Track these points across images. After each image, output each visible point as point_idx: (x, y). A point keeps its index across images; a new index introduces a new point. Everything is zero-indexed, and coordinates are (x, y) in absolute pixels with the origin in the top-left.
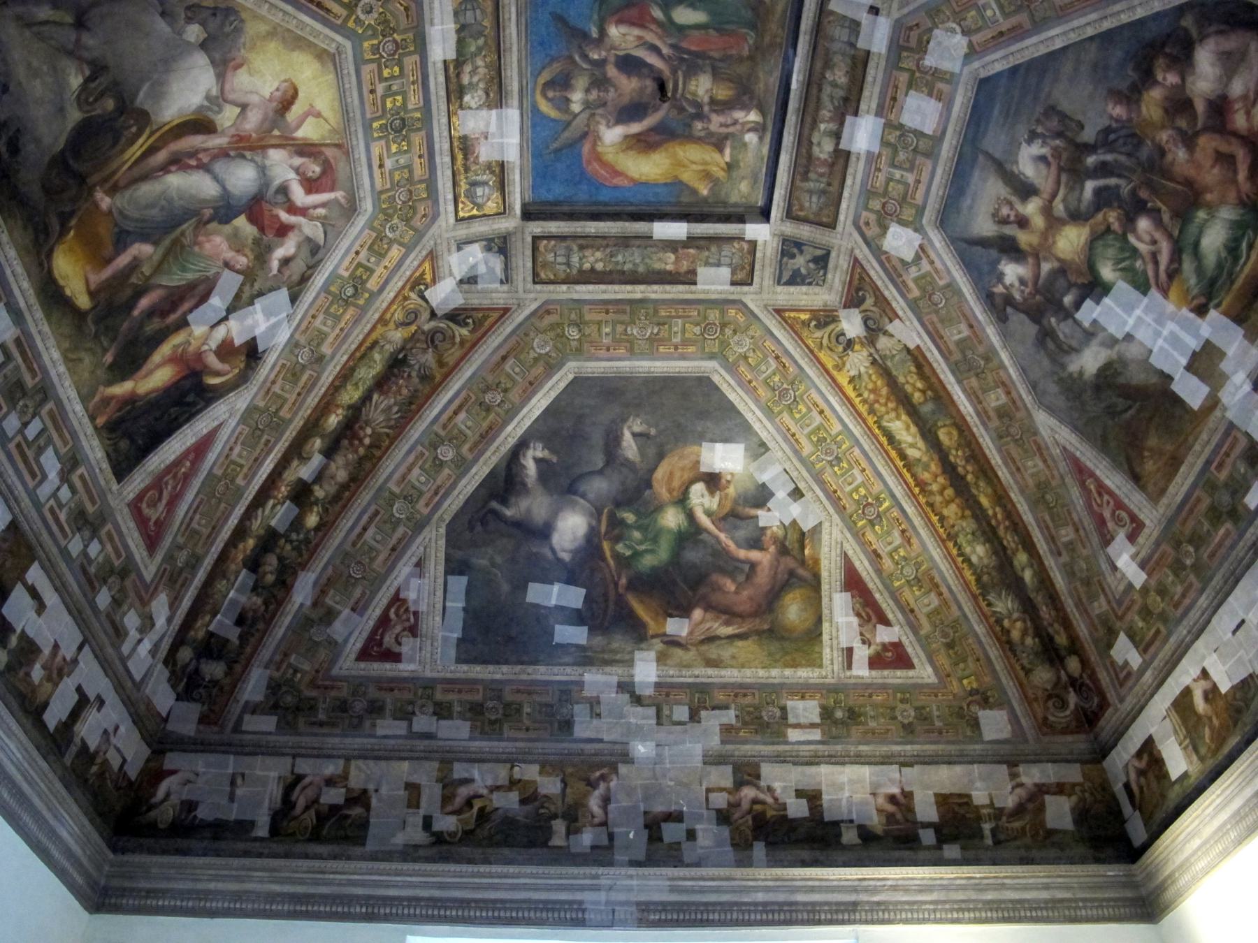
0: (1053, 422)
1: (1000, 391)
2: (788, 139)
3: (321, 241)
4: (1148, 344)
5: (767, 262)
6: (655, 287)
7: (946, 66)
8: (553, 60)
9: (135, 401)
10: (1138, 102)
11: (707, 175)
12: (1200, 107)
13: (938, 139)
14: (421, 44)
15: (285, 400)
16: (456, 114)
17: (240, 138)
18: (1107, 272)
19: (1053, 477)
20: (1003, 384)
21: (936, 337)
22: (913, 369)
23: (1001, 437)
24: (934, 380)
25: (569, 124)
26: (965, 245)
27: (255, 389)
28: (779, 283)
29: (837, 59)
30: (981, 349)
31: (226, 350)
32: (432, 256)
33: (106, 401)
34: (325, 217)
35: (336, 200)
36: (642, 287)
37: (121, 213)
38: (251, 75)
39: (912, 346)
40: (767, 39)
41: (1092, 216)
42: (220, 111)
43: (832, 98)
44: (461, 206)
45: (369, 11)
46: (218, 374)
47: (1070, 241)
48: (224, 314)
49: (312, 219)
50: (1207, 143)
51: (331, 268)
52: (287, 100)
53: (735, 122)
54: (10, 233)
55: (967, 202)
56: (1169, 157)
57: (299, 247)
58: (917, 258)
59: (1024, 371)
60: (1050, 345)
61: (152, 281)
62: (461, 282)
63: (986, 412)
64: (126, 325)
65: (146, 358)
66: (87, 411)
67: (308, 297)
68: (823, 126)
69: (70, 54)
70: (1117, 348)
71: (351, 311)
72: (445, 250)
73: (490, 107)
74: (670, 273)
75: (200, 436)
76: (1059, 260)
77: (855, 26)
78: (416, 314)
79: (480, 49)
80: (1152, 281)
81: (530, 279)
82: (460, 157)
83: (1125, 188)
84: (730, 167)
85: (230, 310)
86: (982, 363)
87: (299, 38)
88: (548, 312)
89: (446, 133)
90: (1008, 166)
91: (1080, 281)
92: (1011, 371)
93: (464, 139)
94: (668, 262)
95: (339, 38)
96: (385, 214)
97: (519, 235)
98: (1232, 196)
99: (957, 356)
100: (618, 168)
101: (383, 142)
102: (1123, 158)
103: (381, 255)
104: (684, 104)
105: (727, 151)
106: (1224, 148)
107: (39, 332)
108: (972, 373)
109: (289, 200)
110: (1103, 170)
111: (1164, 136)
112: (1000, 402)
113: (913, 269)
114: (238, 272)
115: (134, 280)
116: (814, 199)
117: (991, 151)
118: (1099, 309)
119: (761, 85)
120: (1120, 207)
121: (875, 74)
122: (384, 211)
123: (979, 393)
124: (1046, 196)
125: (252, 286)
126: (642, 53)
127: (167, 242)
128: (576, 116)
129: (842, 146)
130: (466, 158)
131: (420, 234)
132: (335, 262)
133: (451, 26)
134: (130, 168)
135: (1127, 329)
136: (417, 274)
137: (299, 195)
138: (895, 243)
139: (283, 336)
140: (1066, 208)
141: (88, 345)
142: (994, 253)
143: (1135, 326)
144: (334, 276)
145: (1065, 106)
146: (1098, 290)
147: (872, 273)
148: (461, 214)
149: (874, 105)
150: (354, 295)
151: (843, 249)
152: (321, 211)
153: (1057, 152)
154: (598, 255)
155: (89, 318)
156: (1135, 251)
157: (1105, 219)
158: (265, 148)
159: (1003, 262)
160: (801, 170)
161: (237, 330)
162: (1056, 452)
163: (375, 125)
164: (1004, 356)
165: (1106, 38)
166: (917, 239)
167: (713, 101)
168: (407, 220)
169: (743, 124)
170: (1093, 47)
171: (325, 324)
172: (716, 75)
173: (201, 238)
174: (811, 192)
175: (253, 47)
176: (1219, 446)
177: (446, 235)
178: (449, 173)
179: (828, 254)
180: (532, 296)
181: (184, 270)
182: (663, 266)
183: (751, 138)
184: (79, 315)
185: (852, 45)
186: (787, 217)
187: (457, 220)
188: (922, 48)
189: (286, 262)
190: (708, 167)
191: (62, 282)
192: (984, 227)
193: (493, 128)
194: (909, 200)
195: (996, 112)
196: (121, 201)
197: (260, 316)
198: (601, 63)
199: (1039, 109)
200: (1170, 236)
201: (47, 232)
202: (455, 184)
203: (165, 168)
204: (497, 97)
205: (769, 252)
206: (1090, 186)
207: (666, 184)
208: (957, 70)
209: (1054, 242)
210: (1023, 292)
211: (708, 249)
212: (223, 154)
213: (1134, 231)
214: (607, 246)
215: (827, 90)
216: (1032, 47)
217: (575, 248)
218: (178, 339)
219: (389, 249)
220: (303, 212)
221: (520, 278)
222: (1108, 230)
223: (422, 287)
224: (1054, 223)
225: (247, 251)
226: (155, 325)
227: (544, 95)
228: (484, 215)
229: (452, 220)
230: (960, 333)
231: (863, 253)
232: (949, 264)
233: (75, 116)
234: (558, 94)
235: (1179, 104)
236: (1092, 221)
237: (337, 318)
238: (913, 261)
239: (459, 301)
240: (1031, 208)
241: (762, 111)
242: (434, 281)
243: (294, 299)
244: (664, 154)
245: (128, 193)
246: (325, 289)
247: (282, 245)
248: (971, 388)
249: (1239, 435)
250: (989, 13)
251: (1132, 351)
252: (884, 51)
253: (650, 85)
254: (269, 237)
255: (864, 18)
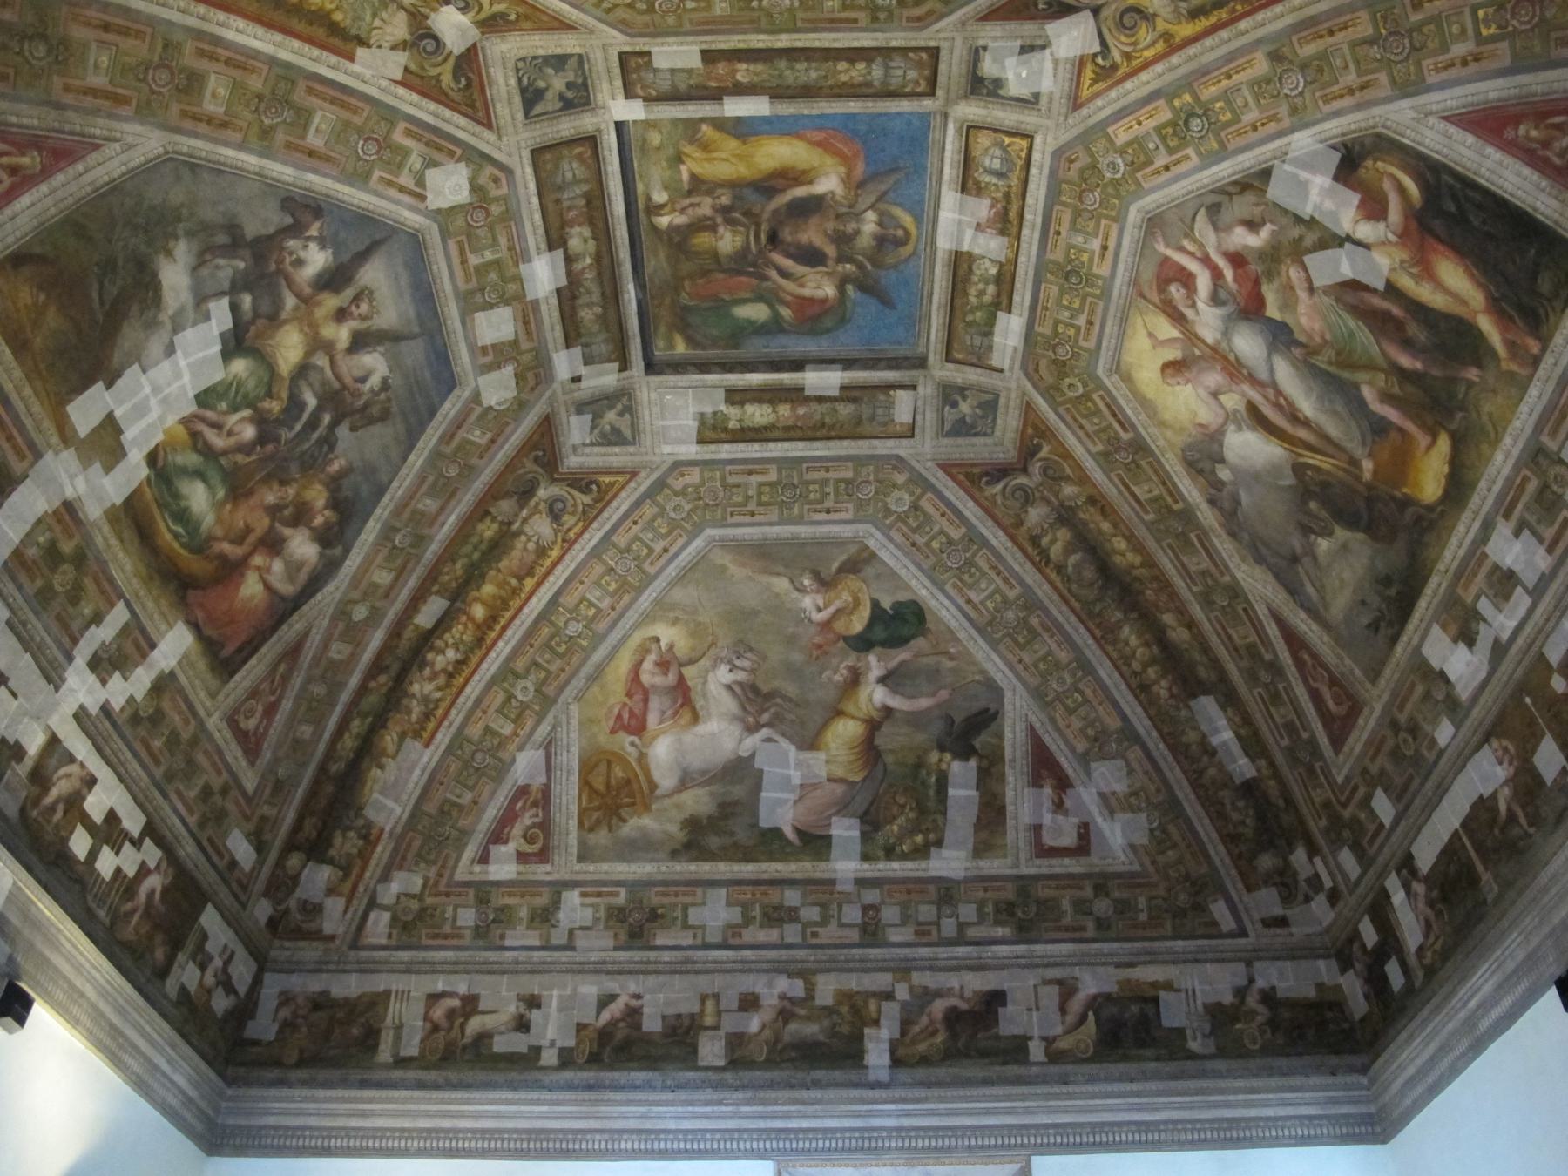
0: (137, 158)
1: (221, 110)
2: (621, 233)
3: (1202, 216)
4: (152, 373)
5: (604, 76)
6: (761, 45)
7: (493, 376)
8: (895, 266)
9: (1495, 300)
10: (327, 486)
11: (706, 147)
12: (287, 531)
13: (466, 314)
14: (1029, 336)
15: (1354, 45)
16: (1008, 260)
17: (1231, 375)
18: (240, 366)
19: (67, 88)
20: (224, 125)
21: (341, 95)
22: (338, 17)
23: (166, 46)
24: (301, 27)
25: (880, 199)
26: (378, 237)
27: (1376, 111)
28: (580, 56)
29: (596, 328)
30: (280, 137)
31: (1373, 208)
32: (1076, 103)
33: (1511, 345)
34: (1186, 235)
35: (1167, 245)
36: (779, 45)
37: (1364, 444)
38: (1196, 414)
39: (361, 52)
40: (667, 301)
41: (290, 388)
42: (1236, 411)
43: (589, 292)
44: (1023, 155)
45: (1070, 385)
46: (1401, 190)
47: (289, 347)
48: (1347, 245)
49: (1201, 246)
50: (261, 523)
51: (1206, 173)
52: (1173, 368)
53: (683, 211)
54: (1435, 561)
55: (404, 280)
56: (276, 487)
57: (1229, 229)
58: (421, 183)
59: (219, 170)
60: (222, 239)
61: (1385, 365)
62: (1044, 47)
63: (212, 57)
64: (1436, 372)
65: (1448, 317)
66: (1530, 378)
67: (1246, 161)
68: (588, 261)
69: (1315, 558)
70: (169, 326)
71: (1208, 92)
72: (1055, 105)
73: (970, 255)
74: (740, 61)
75: (1481, 142)
76: (285, 322)
77: (588, 361)
78: (1121, 25)
79: (972, 311)
80: (202, 412)
81: (944, 54)
82: (1013, 214)
83: (286, 434)
84: (678, 159)
85: (1341, 241)
86: (267, 122)
87: (1142, 404)
88: (919, 19)
89: (1024, 245)
90: (388, 345)
91: (253, 328)
92: (230, 153)
93: (1002, 232)
94: (743, 71)
95: (1106, 381)
96: (1120, 191)
97: (953, 95)
98: (219, 532)
99: (300, 96)
100: (820, 150)
101: (1095, 270)
102: (306, 446)
103: (1138, 142)
104: (744, 220)
105: (685, 176)
106: (252, 538)
107: (1489, 490)
108: (267, 93)
109: (1215, 285)
110: (313, 424)
111: (291, 491)
112: (208, 94)
113: (418, 166)
114: (1306, 270)
115: (1396, 390)
116: (569, 175)
117: (412, 343)
118: (216, 332)
119: (662, 255)
120: (277, 420)
121: (553, 330)
122: (1118, 196)
123: (237, 73)
124: (339, 357)
125: (1301, 238)
126: (800, 269)
127: (1346, 375)
128: (872, 207)
129: (559, 253)
130: (1006, 210)
131: (1085, 138)
132: (1198, 176)
133: (997, 339)
134: (1333, 457)
135: (179, 353)
136: (1101, 86)
137: (1203, 282)
138: (454, 179)
139: (1303, 141)
140: (315, 367)
141: (1474, 415)
142: (346, 257)
143: (176, 364)
144: (1210, 159)
145: (377, 429)
146: (232, 344)
147: (463, 121)
148: (1025, 143)
149: (544, 308)
150: (1191, 115)
151: (511, 130)
152: (1186, 243)
153: (357, 394)
154: (844, 78)
155: (1453, 426)
156: (235, 409)
157: (279, 398)
158: (1214, 349)
159: (331, 258)
160: (598, 203)
161: (1343, 211)
162: (99, 127)
163: (1098, 292)
164: (251, 160)
165: (380, 491)
166: (434, 202)
167: (713, 228)
168: (1093, 166)
169: (673, 210)
170: (385, 479)
171: (1246, 105)
172: (715, 255)
173: (1318, 340)
174: (576, 181)
175: (1182, 429)
176: (21, 428)
177: (1048, 123)
178: (1029, 200)
179: (527, 115)
180: (942, 35)
181: (1352, 334)
182: (752, 67)
183: (660, 197)
184: (1458, 441)
185: (585, 345)
186: (594, 137)
187: (1029, 137)
188: (519, 377)
189: (1252, 225)
190: (705, 156)
191: (1443, 481)
192: (373, 274)
193: (969, 233)
194: (464, 238)
195: (427, 375)
196: (1358, 452)
197: (1314, 196)
198: (841, 259)
199: (394, 409)
200: (225, 453)
201: (1419, 519)
202: (1025, 182)
203: (1305, 423)
204: (961, 263)
205: (605, 86)
206: (311, 401)
207: (756, 134)
208: (481, 380)
209: (301, 331)
210: (291, 254)
211: (691, 87)
212: (1253, 380)
213: (251, 420)
214: (831, 87)
215: (596, 297)
216: (429, 440)
217: (876, 83)
218: (1406, 282)
219: (1129, 144)
220: (1206, 261)
221: (957, 53)
222: (269, 394)
223: (1100, 60)
224: (318, 344)
225: (1284, 279)
226: (1414, 330)
227: (907, 233)
228: (996, 131)
229: (1038, 140)
230: (317, 130)
231: (484, 141)
232: (383, 203)
233: (1341, 533)
234: (892, 232)
235: (300, 515)
236: (287, 384)
237: (1226, 96)
238: (423, 174)
239: (1053, 28)
240: (342, 335)
241: (654, 228)
242: (1081, 63)
243: (1266, 174)
244: (763, 167)
245: (1348, 445)
246: (1222, 153)
247: (1246, 247)
248: (253, 71)
249: (25, 464)
250: (478, 433)
251: (155, 346)
252: (554, 356)
253: (786, 234)
254: (1255, 267)
255: (583, 371)
